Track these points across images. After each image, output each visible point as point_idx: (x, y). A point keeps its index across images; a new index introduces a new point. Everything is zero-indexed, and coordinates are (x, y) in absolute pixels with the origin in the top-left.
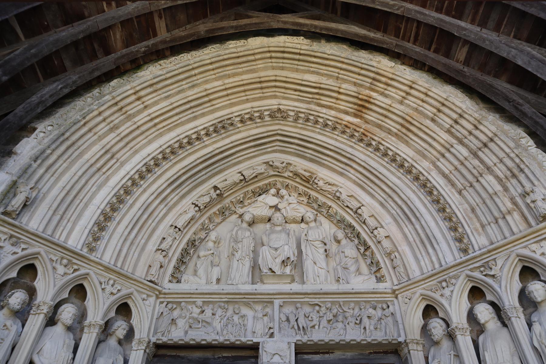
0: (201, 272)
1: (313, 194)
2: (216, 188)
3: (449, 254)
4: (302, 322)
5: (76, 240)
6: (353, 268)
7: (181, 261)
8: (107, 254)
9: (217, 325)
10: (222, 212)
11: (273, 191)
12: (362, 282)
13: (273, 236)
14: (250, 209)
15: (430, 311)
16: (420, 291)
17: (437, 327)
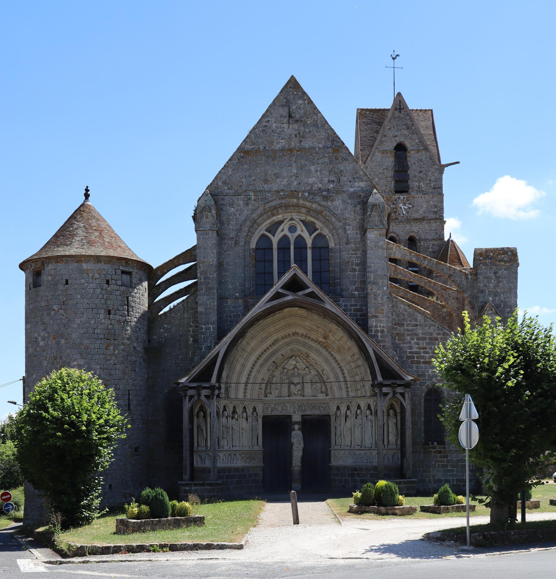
0: (273, 393)
1: (308, 360)
2: (274, 362)
3: (345, 396)
4: (303, 409)
5: (241, 395)
6: (319, 391)
7: (266, 389)
8: (248, 397)
9: (280, 409)
10: (276, 368)
11: (294, 358)
12: (321, 396)
13: (295, 378)
14: (286, 367)
15: (338, 408)
16: (336, 402)
17: (338, 412)
